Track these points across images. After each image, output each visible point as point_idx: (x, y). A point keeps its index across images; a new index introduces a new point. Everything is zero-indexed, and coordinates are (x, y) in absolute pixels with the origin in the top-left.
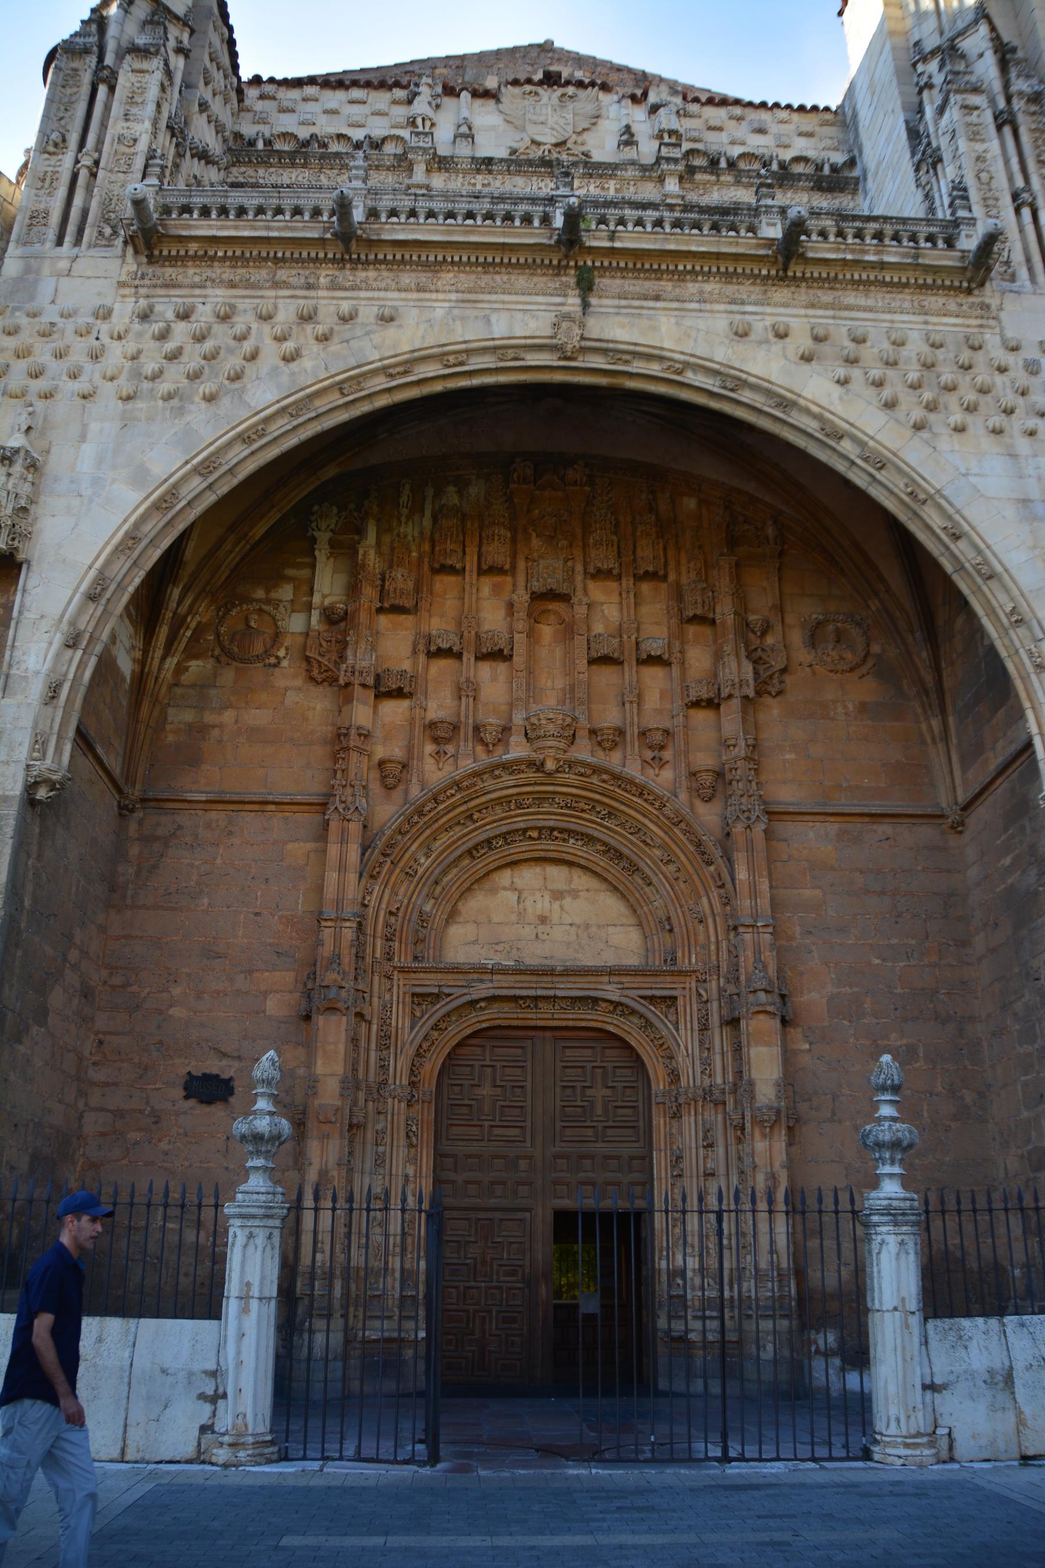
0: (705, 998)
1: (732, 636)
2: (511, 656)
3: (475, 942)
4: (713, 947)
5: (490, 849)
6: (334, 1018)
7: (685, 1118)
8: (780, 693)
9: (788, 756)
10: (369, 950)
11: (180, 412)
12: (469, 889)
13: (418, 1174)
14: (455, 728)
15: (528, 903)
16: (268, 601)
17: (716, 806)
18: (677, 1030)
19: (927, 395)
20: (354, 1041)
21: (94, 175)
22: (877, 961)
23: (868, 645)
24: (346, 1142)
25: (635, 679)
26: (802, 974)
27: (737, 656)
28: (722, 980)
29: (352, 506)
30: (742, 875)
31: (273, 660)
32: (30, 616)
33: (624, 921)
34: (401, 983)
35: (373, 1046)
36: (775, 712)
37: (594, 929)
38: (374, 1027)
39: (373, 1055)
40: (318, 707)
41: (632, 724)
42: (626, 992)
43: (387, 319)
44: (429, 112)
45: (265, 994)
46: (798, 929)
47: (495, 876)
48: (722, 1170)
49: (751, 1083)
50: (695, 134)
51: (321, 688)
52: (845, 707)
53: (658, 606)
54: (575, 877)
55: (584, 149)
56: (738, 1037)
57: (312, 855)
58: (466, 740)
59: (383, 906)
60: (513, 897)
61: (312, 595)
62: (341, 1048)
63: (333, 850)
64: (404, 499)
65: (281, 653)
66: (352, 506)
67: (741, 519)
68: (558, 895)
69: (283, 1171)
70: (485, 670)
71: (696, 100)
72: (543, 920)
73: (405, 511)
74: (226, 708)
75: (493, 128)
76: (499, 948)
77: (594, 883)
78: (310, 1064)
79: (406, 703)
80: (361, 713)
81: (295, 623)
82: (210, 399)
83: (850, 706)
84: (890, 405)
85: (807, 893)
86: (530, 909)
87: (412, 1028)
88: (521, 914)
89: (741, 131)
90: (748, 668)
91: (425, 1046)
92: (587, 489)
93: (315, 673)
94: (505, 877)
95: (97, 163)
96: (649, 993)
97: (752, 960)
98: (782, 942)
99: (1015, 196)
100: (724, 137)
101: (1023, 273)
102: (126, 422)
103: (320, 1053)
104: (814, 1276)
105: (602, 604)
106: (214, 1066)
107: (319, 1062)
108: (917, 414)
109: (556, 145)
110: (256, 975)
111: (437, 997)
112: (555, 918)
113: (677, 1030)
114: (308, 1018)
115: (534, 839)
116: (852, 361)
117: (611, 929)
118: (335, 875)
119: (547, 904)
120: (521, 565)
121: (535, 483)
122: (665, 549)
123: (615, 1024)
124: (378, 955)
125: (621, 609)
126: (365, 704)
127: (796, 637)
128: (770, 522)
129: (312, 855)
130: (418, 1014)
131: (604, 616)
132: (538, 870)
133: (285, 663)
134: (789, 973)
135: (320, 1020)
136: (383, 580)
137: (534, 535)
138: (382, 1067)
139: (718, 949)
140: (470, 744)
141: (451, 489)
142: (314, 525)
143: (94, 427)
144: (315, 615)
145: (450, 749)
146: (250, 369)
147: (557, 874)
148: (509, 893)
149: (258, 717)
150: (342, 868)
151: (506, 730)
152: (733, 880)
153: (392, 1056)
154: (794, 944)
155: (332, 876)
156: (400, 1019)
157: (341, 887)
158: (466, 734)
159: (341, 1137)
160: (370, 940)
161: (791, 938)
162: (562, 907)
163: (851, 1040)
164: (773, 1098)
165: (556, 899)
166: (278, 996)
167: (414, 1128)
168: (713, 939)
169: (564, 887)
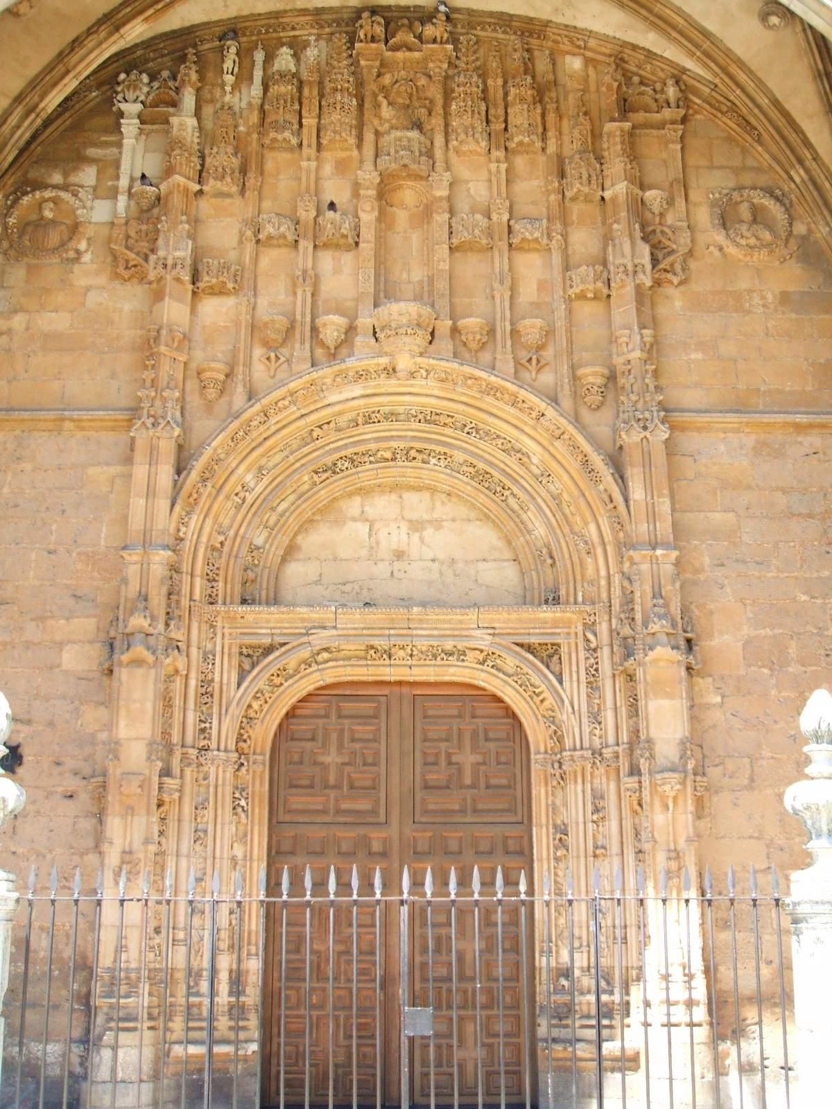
0: (593, 646)
1: (624, 214)
2: (357, 244)
3: (318, 582)
4: (603, 582)
5: (334, 472)
6: (140, 672)
7: (570, 787)
8: (681, 283)
9: (693, 356)
10: (185, 589)
12: (311, 521)
13: (248, 857)
14: (290, 330)
15: (382, 535)
16: (65, 187)
17: (607, 414)
18: (561, 682)
20: (167, 701)
22: (804, 598)
23: (791, 225)
24: (155, 819)
25: (506, 267)
26: (711, 613)
27: (631, 236)
28: (614, 621)
29: (165, 74)
30: (637, 493)
31: (72, 254)
33: (497, 555)
34: (227, 631)
35: (191, 704)
36: (678, 304)
37: (460, 565)
38: (193, 683)
39: (191, 717)
40: (127, 307)
41: (503, 318)
42: (497, 640)
45: (60, 645)
46: (707, 561)
47: (343, 504)
48: (615, 848)
49: (649, 741)
51: (128, 286)
52: (763, 298)
53: (536, 183)
54: (438, 504)
56: (635, 688)
57: (118, 481)
58: (302, 342)
59: (204, 539)
60: (363, 529)
61: (117, 177)
62: (149, 705)
63: (140, 471)
64: (228, 64)
65: (83, 246)
66: (165, 74)
67: (636, 79)
68: (416, 526)
69: (82, 855)
70: (327, 261)
72: (399, 555)
73: (229, 79)
74: (16, 312)
76: (347, 588)
77: (463, 511)
78: (110, 725)
79: (230, 301)
80: (174, 311)
81: (100, 212)
83: (770, 297)
85: (717, 517)
86: (384, 544)
87: (239, 685)
90: (645, 250)
91: (256, 705)
92: (450, 47)
93: (121, 270)
94: (353, 506)
96: (526, 640)
97: (650, 595)
98: (688, 576)
103: (123, 713)
104: (725, 972)
105: (467, 182)
107: (122, 723)
110: (51, 622)
112: (414, 552)
113: (561, 682)
114: (111, 671)
115: (387, 460)
117: (481, 565)
118: (142, 502)
119: (404, 537)
120: (369, 137)
121: (387, 42)
122: (543, 115)
124: (197, 596)
125: (490, 187)
126: (180, 300)
127: (703, 216)
128: (670, 82)
129: (118, 481)
130: (247, 667)
131: (470, 196)
132: (394, 497)
133: (87, 258)
134: (697, 612)
135: (123, 674)
136: (203, 157)
137: (385, 103)
138: (203, 730)
139: (609, 584)
140: (307, 345)
141: (285, 52)
142: (120, 97)
144: (122, 200)
145: (285, 351)
147: (417, 504)
148: (359, 525)
149: (56, 321)
150: (150, 493)
151: (351, 330)
152: (626, 501)
153: (215, 717)
154: (702, 577)
156: (225, 673)
157: (149, 515)
158: (302, 334)
159: (148, 813)
160: (186, 579)
161: (697, 571)
162: (422, 540)
163: (773, 692)
164: (677, 761)
165: (417, 530)
166: (76, 647)
167: (243, 803)
168: (603, 573)
169: (426, 517)
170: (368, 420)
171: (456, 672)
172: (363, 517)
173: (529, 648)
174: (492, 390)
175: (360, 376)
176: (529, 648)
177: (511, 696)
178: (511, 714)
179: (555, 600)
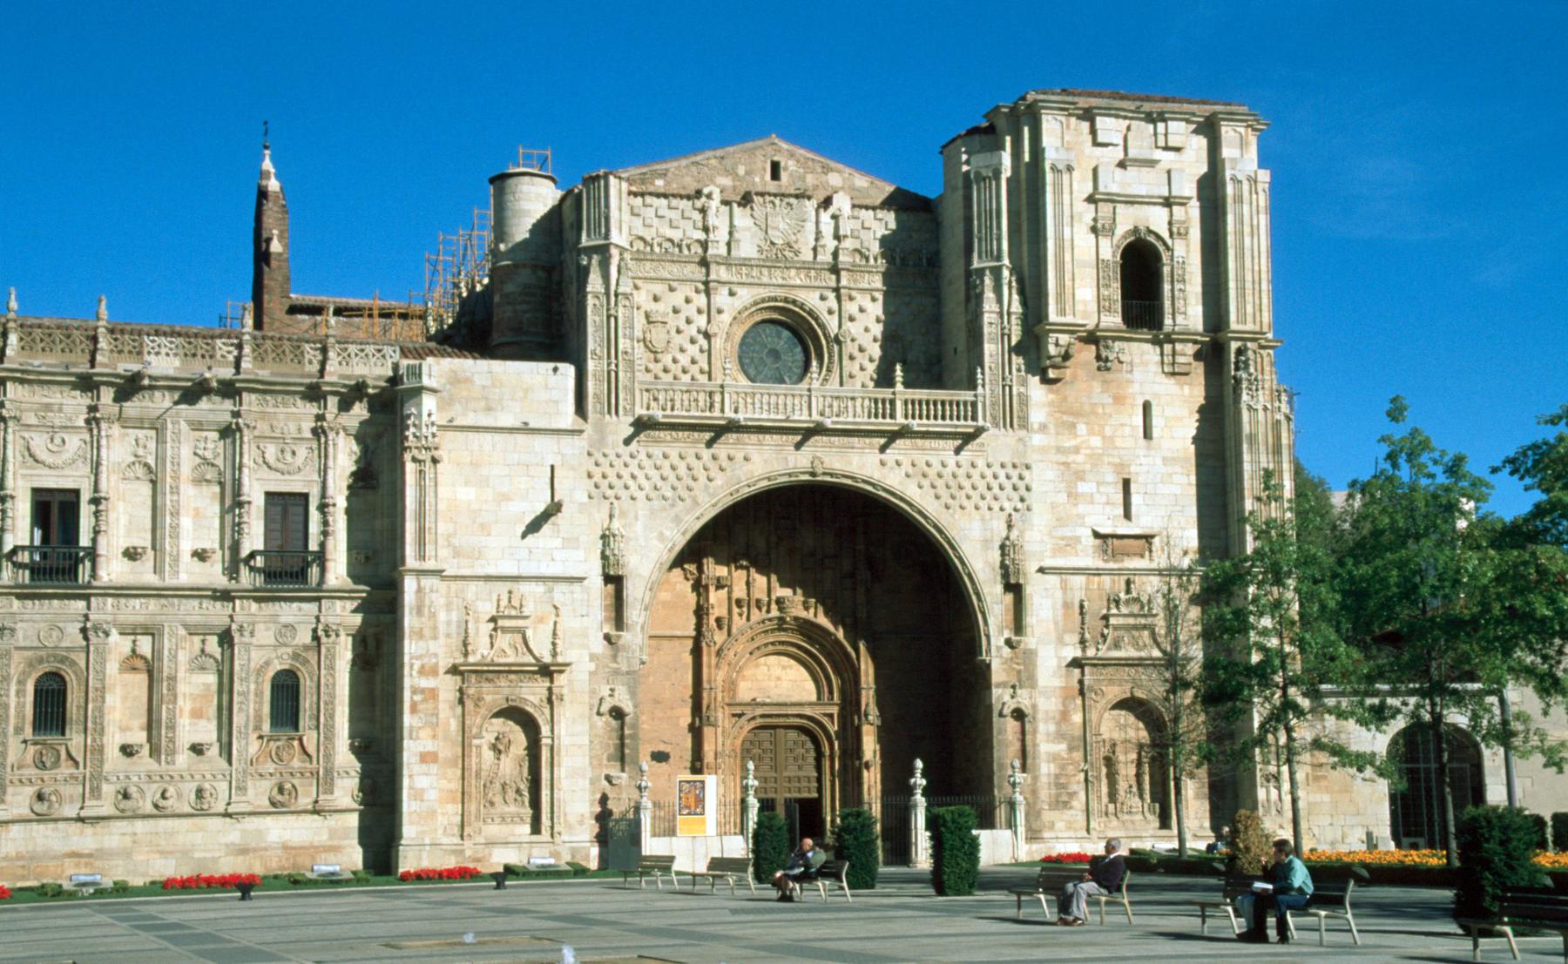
21: (616, 373)
32: (630, 599)
43: (746, 459)
50: (856, 233)
68: (784, 668)
72: (779, 679)
75: (749, 229)
84: (937, 497)
88: (770, 676)
95: (617, 366)
99: (1003, 379)
106: (662, 748)
111: (740, 716)
116: (925, 476)
143: (640, 513)
172: (766, 665)
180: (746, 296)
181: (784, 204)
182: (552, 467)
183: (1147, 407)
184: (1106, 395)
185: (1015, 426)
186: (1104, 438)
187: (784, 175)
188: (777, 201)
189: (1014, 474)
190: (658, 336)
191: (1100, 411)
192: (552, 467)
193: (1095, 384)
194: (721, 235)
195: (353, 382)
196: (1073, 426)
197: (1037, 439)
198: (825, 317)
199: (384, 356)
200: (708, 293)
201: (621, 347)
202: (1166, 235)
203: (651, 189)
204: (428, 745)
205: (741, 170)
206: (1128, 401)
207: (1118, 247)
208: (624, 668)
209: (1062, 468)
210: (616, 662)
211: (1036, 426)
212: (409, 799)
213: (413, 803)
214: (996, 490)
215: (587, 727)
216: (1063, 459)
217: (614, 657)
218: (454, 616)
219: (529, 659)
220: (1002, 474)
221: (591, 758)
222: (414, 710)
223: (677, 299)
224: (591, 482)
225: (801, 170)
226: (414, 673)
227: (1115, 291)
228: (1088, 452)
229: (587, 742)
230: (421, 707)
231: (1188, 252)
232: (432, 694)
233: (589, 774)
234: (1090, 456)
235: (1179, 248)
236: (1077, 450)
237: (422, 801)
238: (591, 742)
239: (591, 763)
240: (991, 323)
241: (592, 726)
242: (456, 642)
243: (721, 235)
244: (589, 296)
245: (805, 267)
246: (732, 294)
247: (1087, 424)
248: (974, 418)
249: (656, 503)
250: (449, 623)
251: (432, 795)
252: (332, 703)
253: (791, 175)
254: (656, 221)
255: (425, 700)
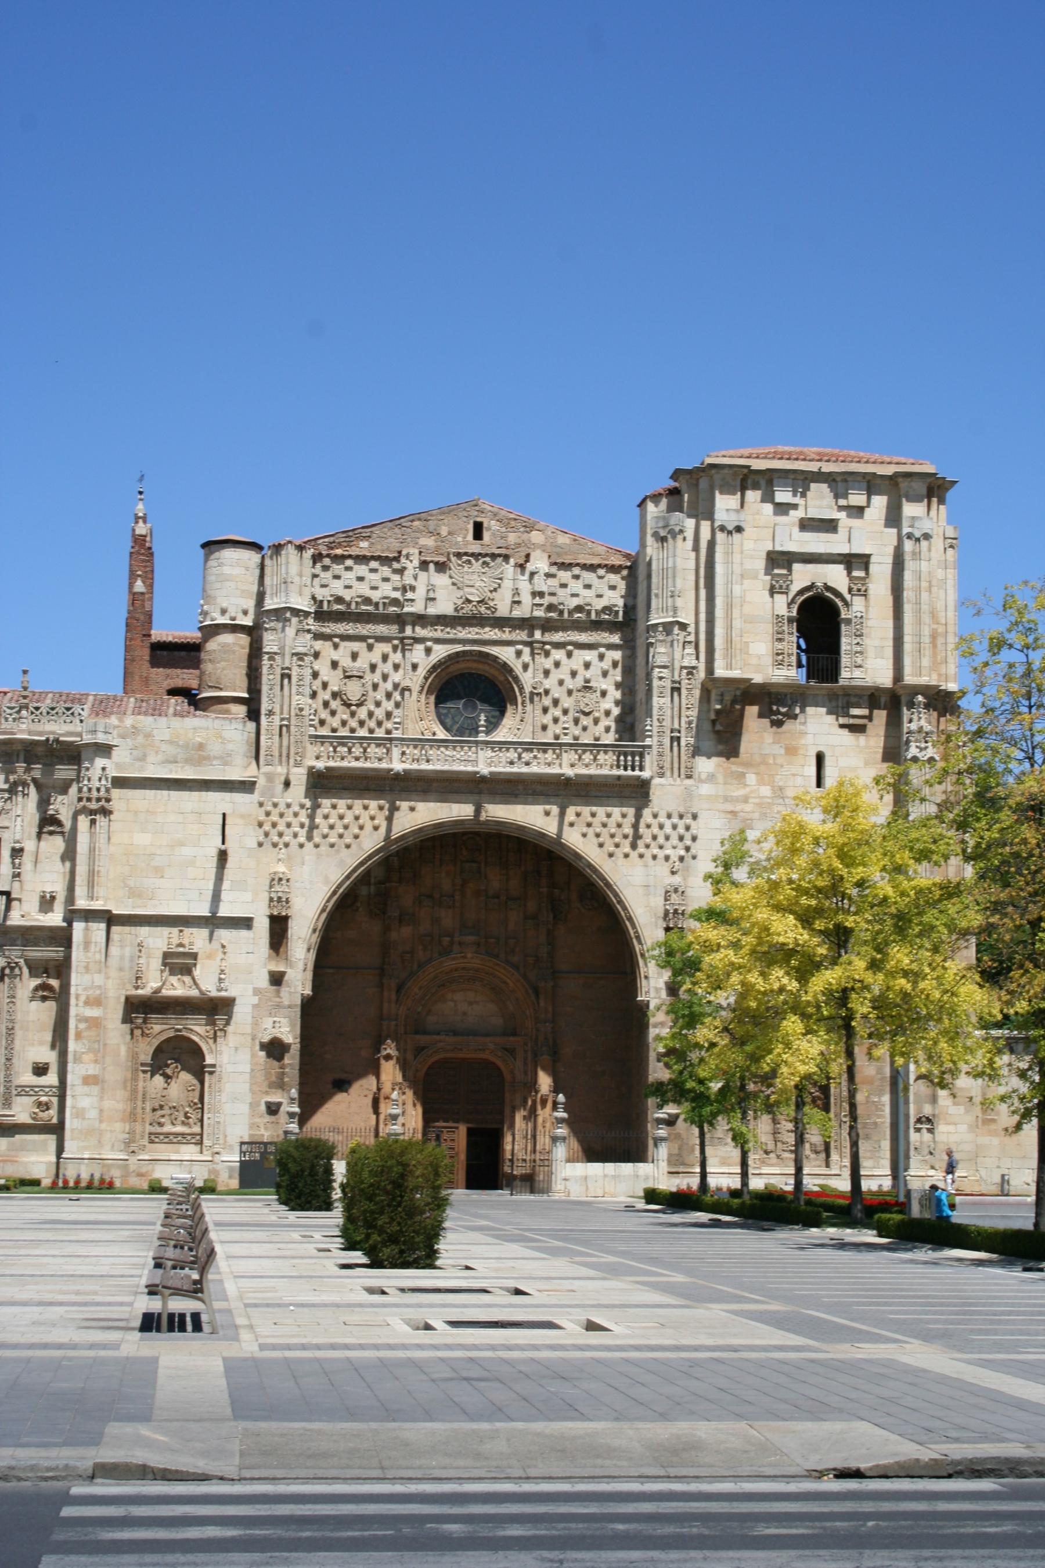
11: (338, 851)
19: (617, 840)
30: (542, 1004)
44: (413, 583)
50: (552, 590)
55: (492, 604)
63: (386, 994)
68: (470, 1003)
71: (555, 564)
72: (465, 1013)
75: (446, 587)
80: (394, 935)
82: (348, 846)
84: (601, 845)
89: (576, 586)
90: (551, 916)
100: (568, 591)
101: (668, 773)
102: (319, 856)
108: (612, 849)
109: (479, 602)
116: (589, 825)
123: (493, 1059)
143: (307, 858)
146: (362, 833)
151: (452, 943)
155: (386, 1005)
170: (456, 970)
171: (482, 1055)
173: (506, 1049)
174: (497, 964)
175: (454, 959)
176: (506, 1049)
177: (499, 1063)
178: (499, 1069)
179: (514, 1034)
180: (441, 652)
181: (481, 562)
182: (224, 815)
183: (820, 759)
184: (778, 746)
185: (683, 776)
186: (773, 787)
187: (486, 536)
188: (473, 561)
189: (681, 824)
190: (353, 690)
191: (771, 762)
192: (224, 815)
193: (766, 735)
194: (420, 594)
195: (44, 738)
196: (742, 775)
197: (705, 789)
198: (518, 669)
199: (72, 714)
200: (403, 651)
201: (294, 703)
202: (844, 591)
203: (354, 551)
204: (92, 1069)
205: (444, 531)
206: (801, 752)
207: (793, 601)
208: (286, 1003)
209: (729, 816)
210: (279, 997)
211: (703, 776)
212: (72, 1118)
213: (75, 1120)
214: (661, 840)
215: (248, 1057)
216: (729, 807)
217: (278, 992)
218: (127, 951)
219: (194, 993)
220: (668, 824)
221: (251, 1084)
222: (78, 1036)
223: (375, 656)
224: (261, 832)
225: (504, 530)
226: (81, 1004)
227: (792, 642)
228: (757, 801)
229: (249, 1071)
230: (85, 1034)
231: (867, 607)
232: (95, 1023)
233: (249, 1099)
234: (759, 805)
235: (858, 604)
236: (745, 800)
237: (84, 1119)
238: (252, 1070)
239: (251, 1089)
240: (661, 678)
241: (253, 1055)
242: (129, 975)
243: (420, 594)
244: (266, 657)
245: (500, 623)
246: (428, 651)
247: (757, 774)
248: (641, 769)
249: (324, 848)
250: (122, 958)
251: (93, 1114)
252: (13, 1028)
253: (493, 534)
254: (356, 584)
255: (89, 1028)
